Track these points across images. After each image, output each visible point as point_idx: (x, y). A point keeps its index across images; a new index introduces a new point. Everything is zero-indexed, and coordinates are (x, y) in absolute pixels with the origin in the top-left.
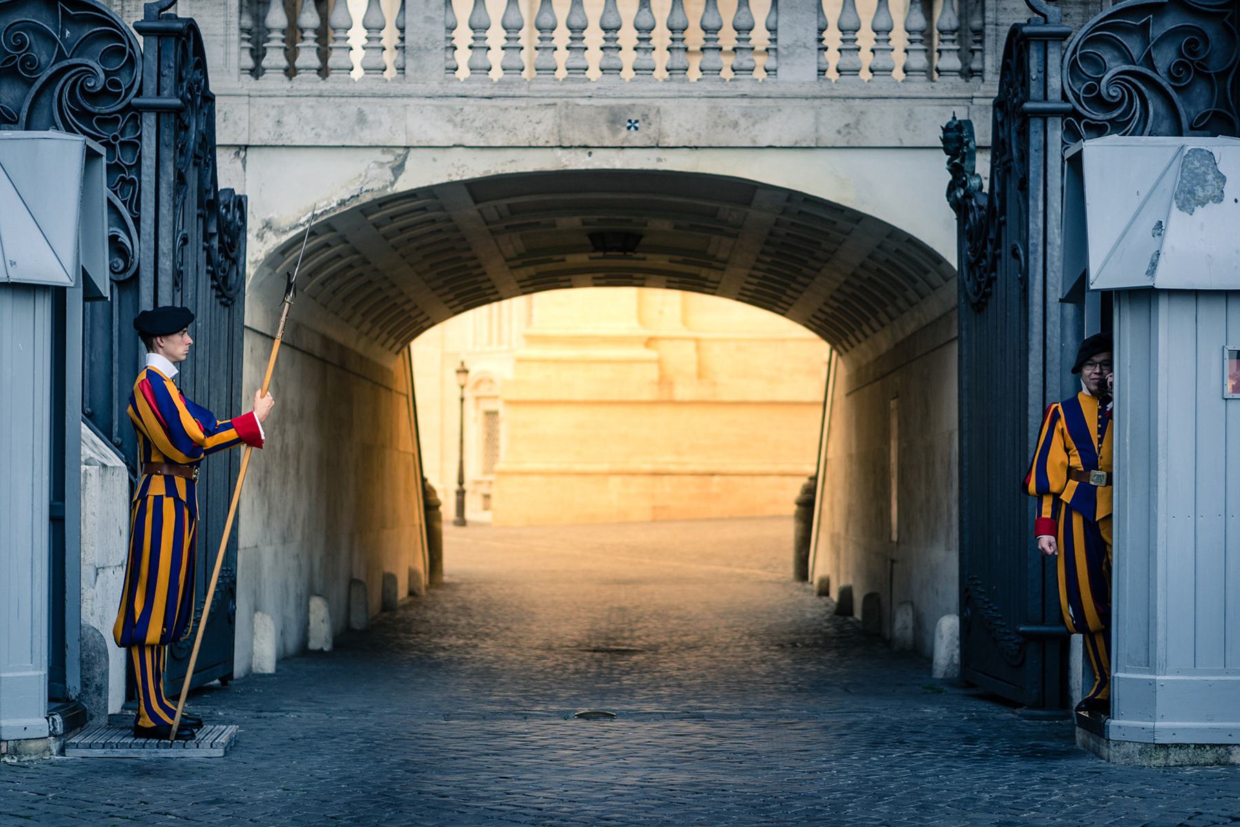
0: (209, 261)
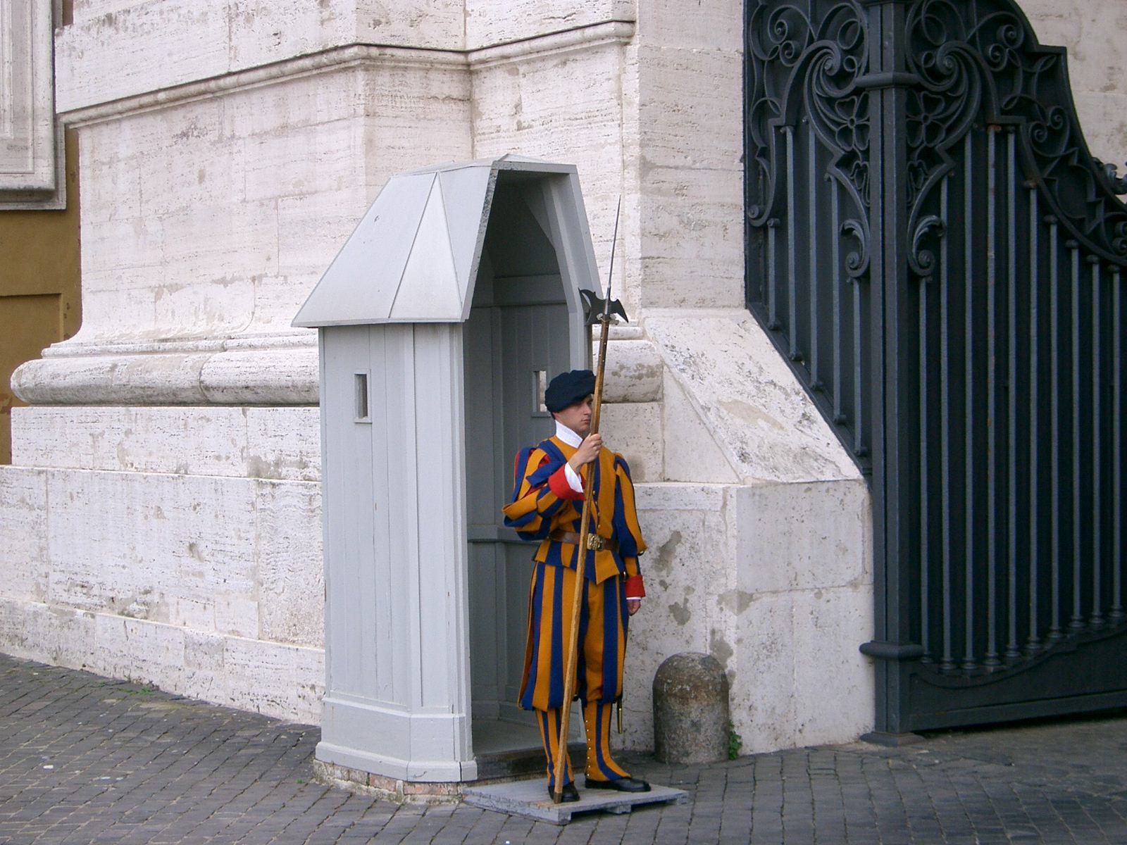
0: (1063, 235)
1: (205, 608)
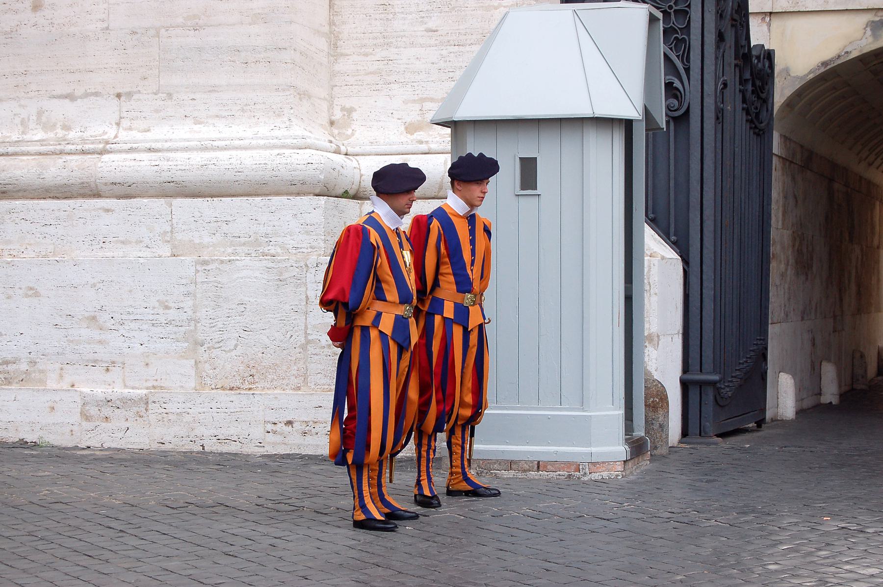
0: (744, 101)
1: (108, 370)
